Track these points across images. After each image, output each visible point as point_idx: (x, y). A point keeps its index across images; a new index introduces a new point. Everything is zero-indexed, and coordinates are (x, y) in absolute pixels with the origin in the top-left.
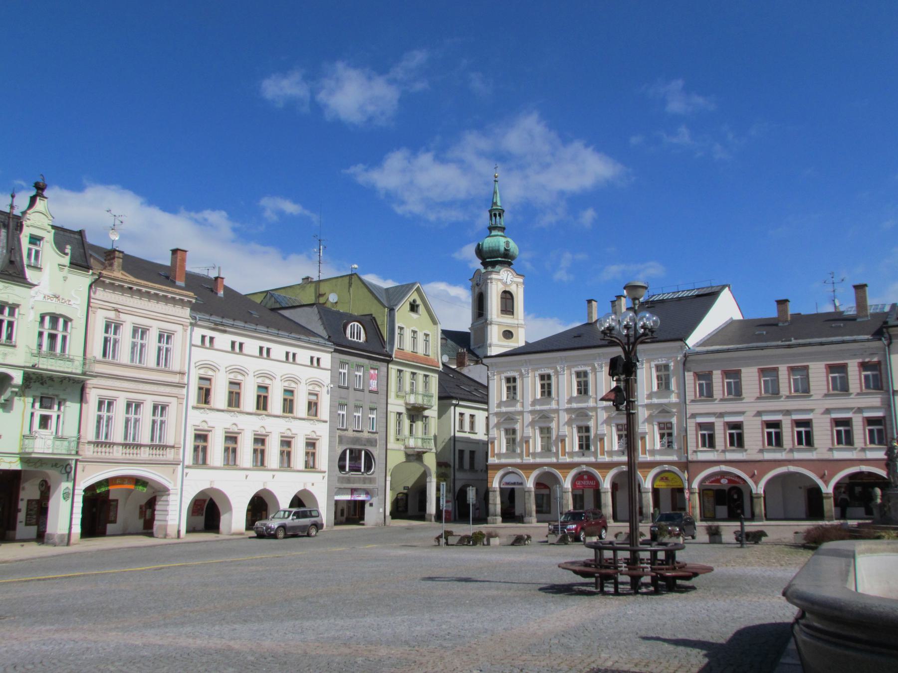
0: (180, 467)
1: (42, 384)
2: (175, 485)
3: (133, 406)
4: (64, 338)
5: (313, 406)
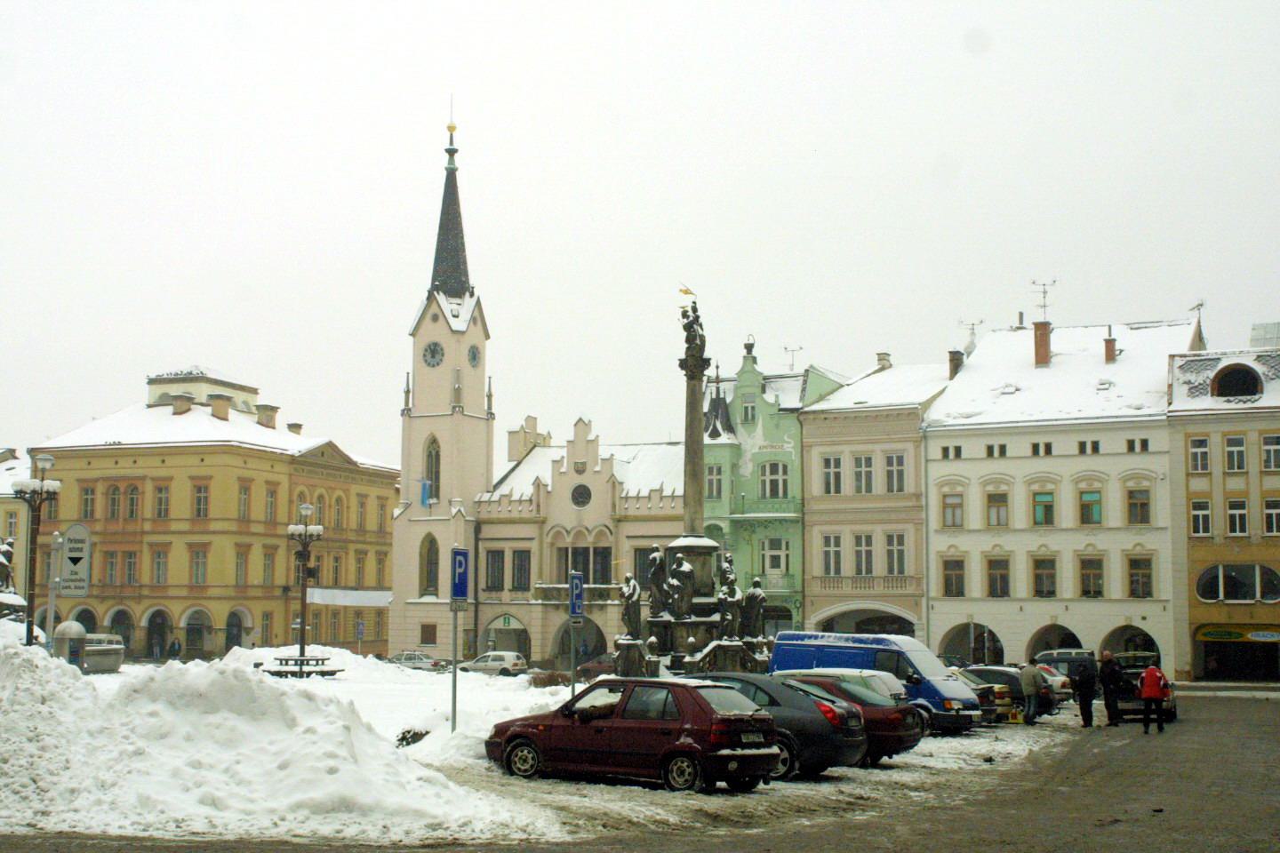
0: (924, 601)
1: (766, 527)
2: (920, 619)
3: (864, 540)
4: (785, 482)
5: (1139, 509)
